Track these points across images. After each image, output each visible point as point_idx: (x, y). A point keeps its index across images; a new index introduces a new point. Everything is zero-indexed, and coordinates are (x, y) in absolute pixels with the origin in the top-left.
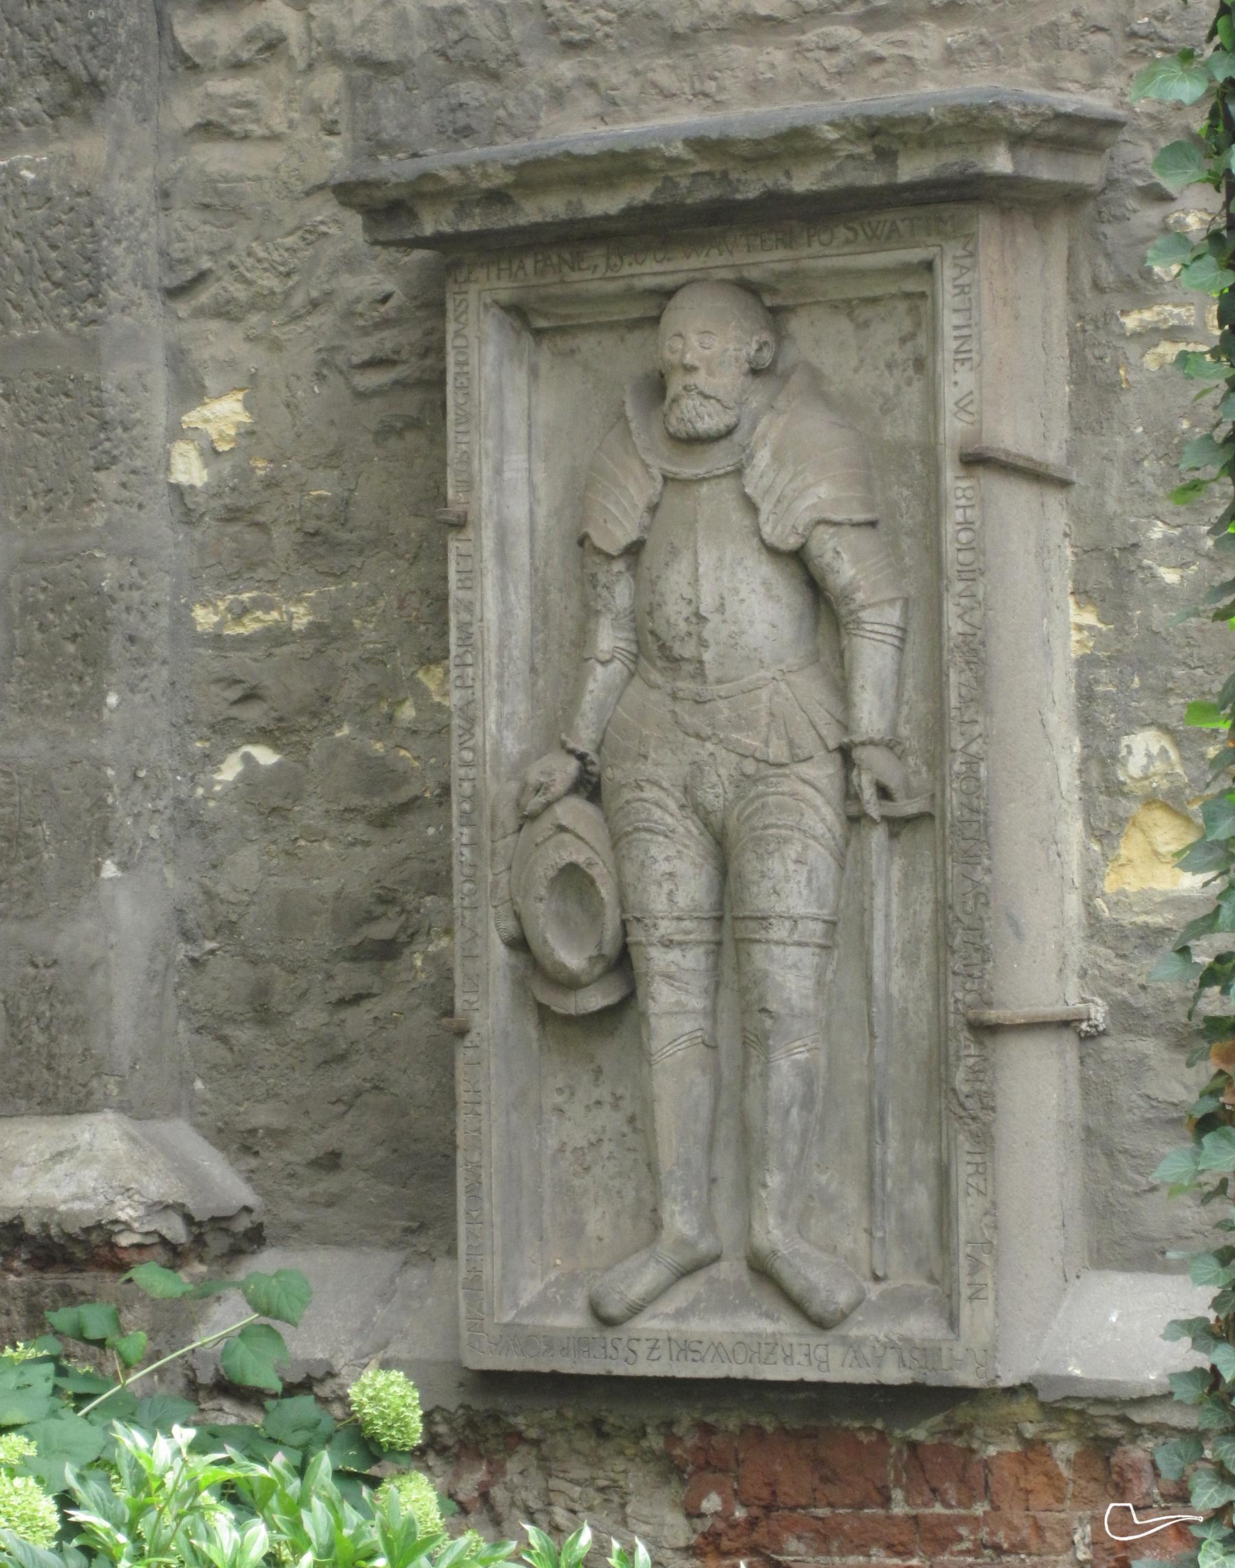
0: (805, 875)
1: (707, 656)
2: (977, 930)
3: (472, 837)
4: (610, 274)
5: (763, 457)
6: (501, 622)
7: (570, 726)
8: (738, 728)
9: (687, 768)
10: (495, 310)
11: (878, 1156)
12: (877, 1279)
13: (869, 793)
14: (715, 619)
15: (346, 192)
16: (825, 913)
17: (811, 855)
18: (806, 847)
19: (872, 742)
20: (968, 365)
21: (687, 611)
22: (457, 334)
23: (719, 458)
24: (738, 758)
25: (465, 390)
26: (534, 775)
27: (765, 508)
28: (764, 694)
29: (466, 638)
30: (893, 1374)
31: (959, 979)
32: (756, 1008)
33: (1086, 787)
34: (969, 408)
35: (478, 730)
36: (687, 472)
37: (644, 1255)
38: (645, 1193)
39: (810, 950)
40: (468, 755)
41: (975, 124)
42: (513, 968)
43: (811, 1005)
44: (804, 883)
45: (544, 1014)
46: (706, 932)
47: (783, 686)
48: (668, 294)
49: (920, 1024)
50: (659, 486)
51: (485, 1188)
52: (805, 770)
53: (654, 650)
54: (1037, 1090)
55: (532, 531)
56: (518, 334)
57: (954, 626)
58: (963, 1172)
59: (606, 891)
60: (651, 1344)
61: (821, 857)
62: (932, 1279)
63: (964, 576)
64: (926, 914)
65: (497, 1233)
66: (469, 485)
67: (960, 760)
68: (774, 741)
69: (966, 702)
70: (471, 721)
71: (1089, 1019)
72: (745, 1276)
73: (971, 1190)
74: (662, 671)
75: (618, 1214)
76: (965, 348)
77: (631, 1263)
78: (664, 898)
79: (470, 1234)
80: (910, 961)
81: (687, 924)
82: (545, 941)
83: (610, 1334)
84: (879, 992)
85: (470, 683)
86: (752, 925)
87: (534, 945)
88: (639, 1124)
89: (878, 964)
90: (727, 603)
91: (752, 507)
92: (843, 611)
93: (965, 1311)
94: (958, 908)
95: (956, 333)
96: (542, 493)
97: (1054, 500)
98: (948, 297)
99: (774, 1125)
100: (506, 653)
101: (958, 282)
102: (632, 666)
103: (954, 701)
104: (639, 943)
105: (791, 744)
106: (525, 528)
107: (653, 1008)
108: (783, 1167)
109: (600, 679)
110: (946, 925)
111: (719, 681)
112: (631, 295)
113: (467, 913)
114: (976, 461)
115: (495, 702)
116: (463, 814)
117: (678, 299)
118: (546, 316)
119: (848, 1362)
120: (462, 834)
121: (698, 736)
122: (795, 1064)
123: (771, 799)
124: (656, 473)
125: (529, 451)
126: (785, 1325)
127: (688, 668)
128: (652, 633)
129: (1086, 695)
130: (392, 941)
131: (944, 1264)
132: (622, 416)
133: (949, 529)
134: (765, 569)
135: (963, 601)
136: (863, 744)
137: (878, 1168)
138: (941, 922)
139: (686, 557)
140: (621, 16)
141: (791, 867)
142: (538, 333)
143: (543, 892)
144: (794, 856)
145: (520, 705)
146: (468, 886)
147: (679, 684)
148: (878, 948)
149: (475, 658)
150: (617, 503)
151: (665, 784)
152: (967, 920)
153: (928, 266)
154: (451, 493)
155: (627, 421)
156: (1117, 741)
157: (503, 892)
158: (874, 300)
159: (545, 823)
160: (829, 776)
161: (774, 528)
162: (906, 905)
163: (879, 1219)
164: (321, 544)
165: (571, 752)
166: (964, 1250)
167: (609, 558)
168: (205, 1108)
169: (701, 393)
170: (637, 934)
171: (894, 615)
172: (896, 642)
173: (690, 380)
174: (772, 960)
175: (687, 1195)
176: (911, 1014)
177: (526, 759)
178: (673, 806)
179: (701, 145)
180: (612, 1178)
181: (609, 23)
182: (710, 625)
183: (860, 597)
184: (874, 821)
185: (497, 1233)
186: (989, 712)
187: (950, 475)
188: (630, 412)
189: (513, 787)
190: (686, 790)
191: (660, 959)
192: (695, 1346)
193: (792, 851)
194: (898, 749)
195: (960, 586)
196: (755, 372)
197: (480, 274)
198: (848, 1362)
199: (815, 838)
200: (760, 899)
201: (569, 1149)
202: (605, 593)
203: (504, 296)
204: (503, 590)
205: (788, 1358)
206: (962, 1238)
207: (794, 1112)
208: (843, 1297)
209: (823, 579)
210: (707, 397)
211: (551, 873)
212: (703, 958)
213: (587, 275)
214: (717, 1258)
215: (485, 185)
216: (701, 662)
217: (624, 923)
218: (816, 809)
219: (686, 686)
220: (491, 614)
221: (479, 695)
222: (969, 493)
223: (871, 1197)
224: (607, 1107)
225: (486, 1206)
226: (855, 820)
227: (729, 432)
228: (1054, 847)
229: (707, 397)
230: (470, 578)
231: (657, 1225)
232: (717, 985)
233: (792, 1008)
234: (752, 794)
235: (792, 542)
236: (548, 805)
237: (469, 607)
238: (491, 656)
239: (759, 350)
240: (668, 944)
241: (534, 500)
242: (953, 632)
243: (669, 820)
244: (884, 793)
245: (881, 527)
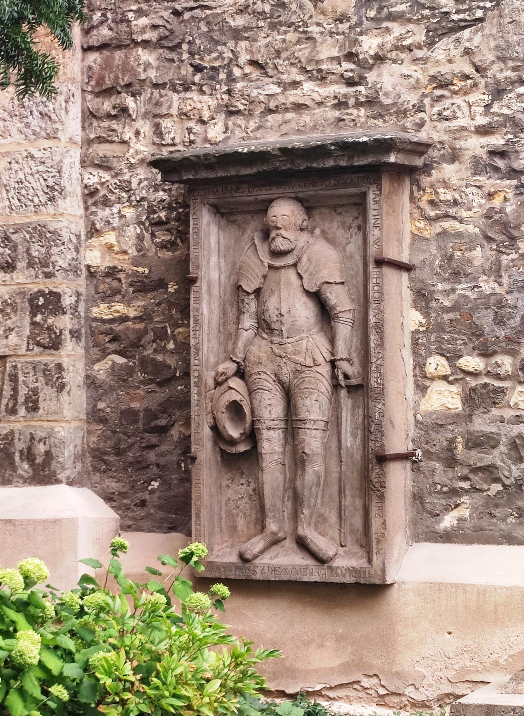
1: (283, 329)
2: (380, 425)
4: (249, 194)
5: (304, 259)
7: (233, 352)
8: (295, 354)
10: (207, 206)
11: (343, 503)
12: (342, 546)
13: (341, 377)
15: (155, 164)
16: (325, 419)
18: (319, 396)
19: (342, 359)
20: (378, 228)
21: (277, 313)
22: (194, 214)
23: (290, 260)
25: (197, 234)
26: (221, 368)
27: (305, 276)
28: (304, 342)
29: (196, 321)
30: (349, 579)
31: (373, 442)
32: (300, 451)
33: (415, 376)
35: (200, 353)
36: (277, 264)
37: (259, 537)
38: (259, 516)
39: (320, 431)
40: (197, 362)
41: (385, 146)
42: (213, 436)
43: (319, 451)
45: (223, 452)
46: (282, 425)
47: (311, 339)
48: (271, 201)
49: (358, 457)
50: (267, 269)
51: (202, 513)
52: (318, 369)
53: (264, 326)
54: (399, 480)
55: (220, 284)
56: (215, 214)
57: (372, 320)
58: (374, 510)
59: (247, 410)
61: (324, 400)
62: (361, 546)
64: (361, 419)
65: (206, 529)
66: (198, 267)
68: (307, 358)
69: (377, 346)
70: (198, 350)
72: (294, 545)
74: (266, 333)
77: (254, 540)
78: (268, 412)
79: (196, 529)
80: (354, 435)
81: (276, 422)
82: (225, 428)
83: (247, 565)
84: (343, 446)
86: (299, 423)
87: (220, 428)
88: (257, 492)
89: (343, 437)
91: (300, 277)
92: (333, 313)
93: (375, 557)
94: (373, 417)
96: (223, 270)
97: (405, 276)
98: (371, 205)
99: (306, 492)
103: (372, 345)
104: (259, 428)
105: (314, 359)
106: (217, 282)
107: (263, 451)
108: (309, 507)
109: (245, 336)
110: (368, 423)
111: (288, 338)
112: (256, 202)
113: (196, 417)
114: (380, 263)
115: (206, 343)
117: (274, 204)
118: (225, 208)
120: (194, 390)
121: (280, 356)
122: (314, 471)
123: (306, 379)
124: (266, 265)
125: (219, 256)
126: (310, 562)
127: (276, 332)
128: (264, 320)
129: (415, 343)
130: (166, 426)
131: (367, 541)
132: (254, 244)
133: (371, 285)
134: (305, 299)
135: (376, 311)
136: (339, 360)
137: (343, 508)
138: (366, 422)
139: (277, 293)
140: (250, 103)
141: (314, 402)
142: (222, 215)
143: (224, 410)
144: (314, 398)
145: (215, 344)
146: (196, 408)
147: (274, 338)
148: (343, 431)
149: (200, 328)
150: (252, 275)
151: (268, 373)
152: (376, 421)
153: (364, 195)
154: (191, 269)
155: (256, 246)
156: (426, 359)
157: (209, 409)
158: (343, 205)
159: (225, 386)
162: (353, 415)
163: (343, 525)
164: (142, 286)
165: (234, 361)
166: (374, 536)
167: (248, 294)
168: (96, 485)
169: (283, 237)
170: (258, 426)
171: (350, 316)
172: (351, 324)
173: (278, 232)
174: (306, 435)
175: (274, 517)
177: (217, 364)
178: (271, 382)
179: (284, 151)
181: (246, 105)
182: (285, 317)
183: (338, 309)
184: (343, 387)
185: (206, 529)
186: (384, 350)
187: (372, 267)
188: (256, 241)
189: (213, 374)
190: (276, 375)
191: (265, 434)
193: (314, 397)
194: (351, 362)
195: (375, 305)
196: (302, 230)
199: (322, 393)
200: (303, 415)
202: (247, 306)
203: (212, 201)
204: (210, 304)
205: (311, 574)
206: (374, 532)
207: (314, 488)
208: (331, 553)
209: (325, 302)
210: (284, 238)
211: (227, 404)
212: (281, 434)
213: (241, 194)
214: (285, 538)
215: (206, 162)
216: (282, 331)
217: (253, 421)
218: (323, 383)
219: (276, 339)
220: (205, 311)
221: (201, 341)
223: (340, 517)
224: (245, 485)
225: (202, 520)
226: (336, 386)
227: (292, 250)
229: (284, 238)
230: (198, 300)
231: (263, 527)
232: (286, 443)
233: (313, 451)
234: (299, 377)
235: (314, 289)
236: (226, 380)
237: (197, 310)
238: (205, 327)
240: (269, 429)
241: (220, 274)
242: (372, 321)
243: (270, 386)
244: (346, 377)
245: (345, 284)
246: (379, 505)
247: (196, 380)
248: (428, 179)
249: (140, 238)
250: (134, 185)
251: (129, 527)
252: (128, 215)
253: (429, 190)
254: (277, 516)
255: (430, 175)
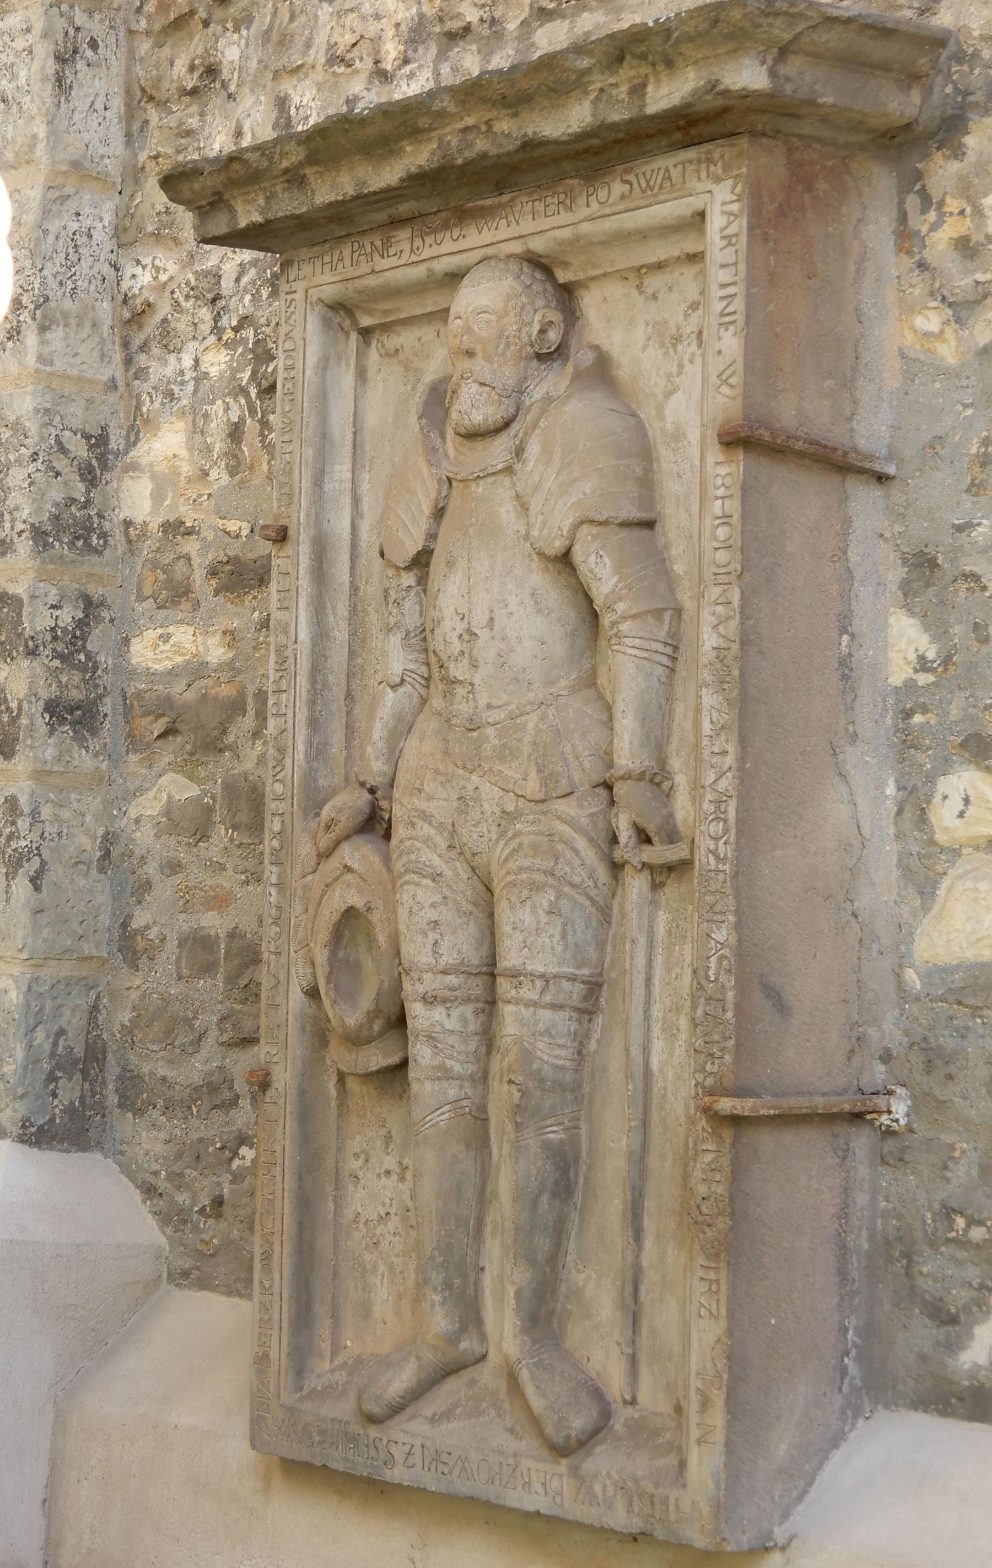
0: (559, 928)
1: (477, 680)
3: (279, 876)
6: (314, 645)
8: (502, 759)
9: (455, 804)
14: (484, 634)
17: (565, 905)
20: (732, 328)
21: (461, 627)
24: (501, 793)
27: (534, 506)
34: (731, 381)
39: (566, 1014)
44: (557, 937)
60: (407, 1448)
63: (722, 579)
67: (709, 797)
71: (890, 1112)
73: (703, 1311)
75: (400, 1297)
76: (731, 309)
85: (283, 710)
90: (496, 617)
95: (722, 293)
96: (366, 504)
100: (319, 678)
101: (725, 233)
102: (423, 691)
106: (346, 544)
116: (274, 852)
118: (370, 312)
119: (581, 1497)
135: (719, 609)
158: (660, 266)
160: (592, 815)
161: (541, 531)
172: (665, 660)
176: (669, 1095)
180: (397, 1256)
192: (445, 1458)
195: (717, 590)
197: (307, 269)
198: (581, 1497)
201: (363, 1220)
205: (527, 1485)
213: (394, 261)
222: (728, 481)
224: (394, 1177)
228: (848, 905)
239: (542, 331)
246: (712, 1275)
247: (275, 843)
248: (954, 166)
249: (235, 433)
250: (227, 285)
251: (186, 1274)
252: (214, 372)
253: (953, 205)
254: (457, 1282)
255: (958, 152)
